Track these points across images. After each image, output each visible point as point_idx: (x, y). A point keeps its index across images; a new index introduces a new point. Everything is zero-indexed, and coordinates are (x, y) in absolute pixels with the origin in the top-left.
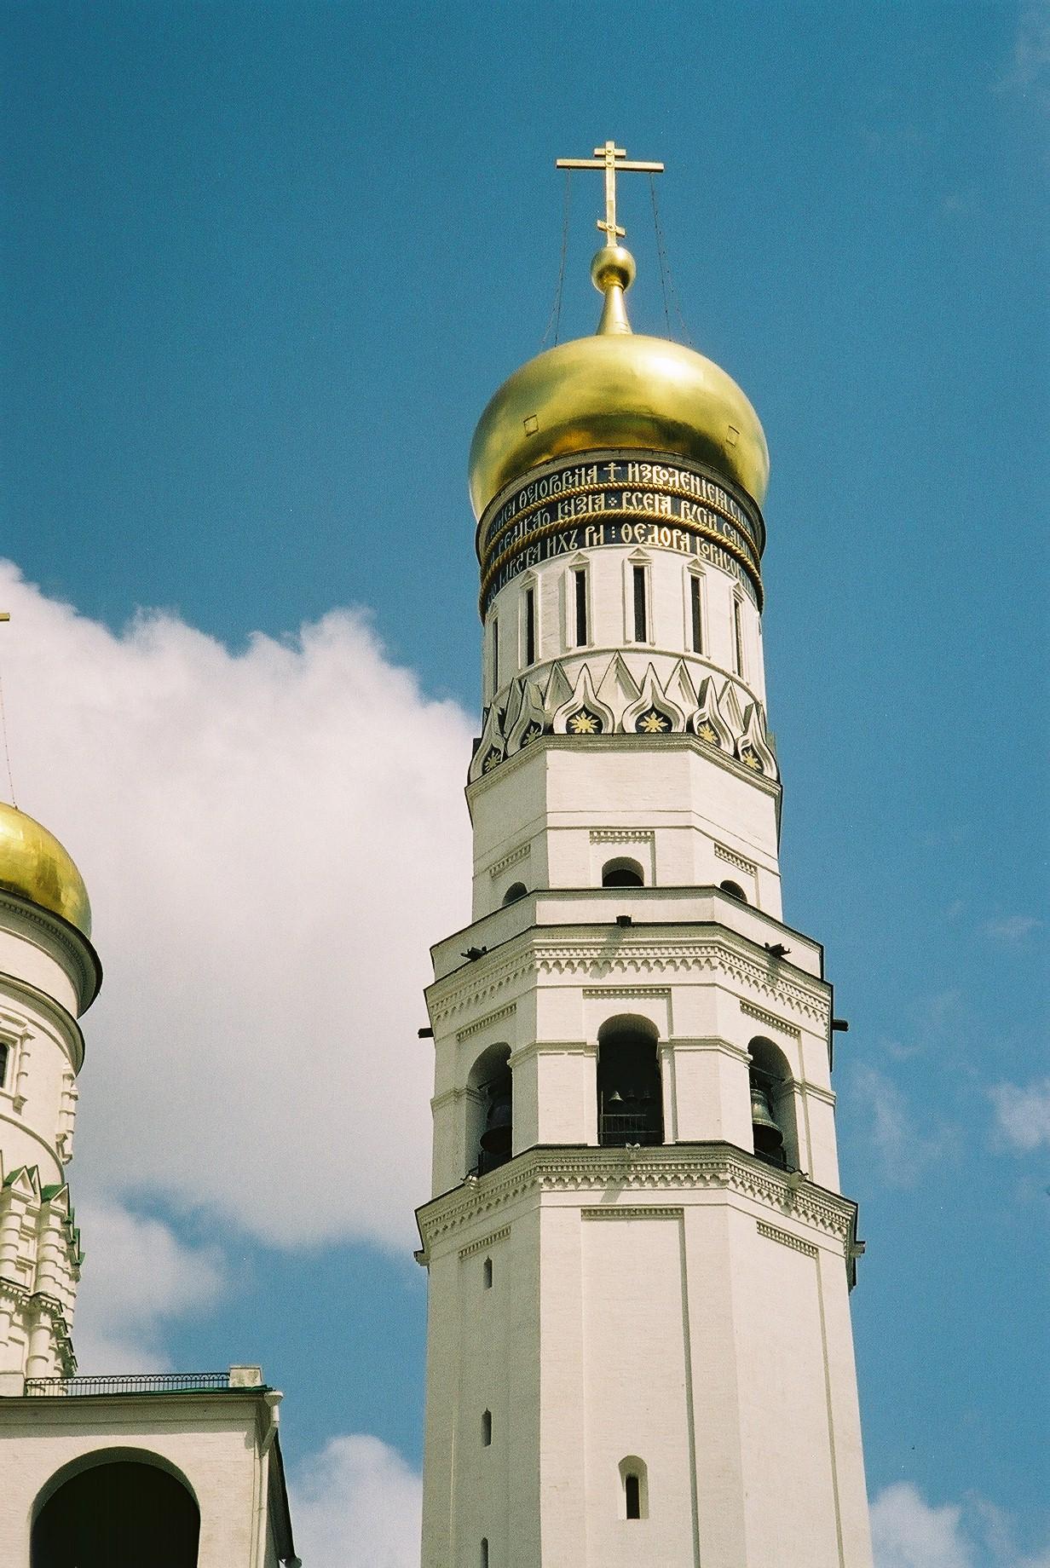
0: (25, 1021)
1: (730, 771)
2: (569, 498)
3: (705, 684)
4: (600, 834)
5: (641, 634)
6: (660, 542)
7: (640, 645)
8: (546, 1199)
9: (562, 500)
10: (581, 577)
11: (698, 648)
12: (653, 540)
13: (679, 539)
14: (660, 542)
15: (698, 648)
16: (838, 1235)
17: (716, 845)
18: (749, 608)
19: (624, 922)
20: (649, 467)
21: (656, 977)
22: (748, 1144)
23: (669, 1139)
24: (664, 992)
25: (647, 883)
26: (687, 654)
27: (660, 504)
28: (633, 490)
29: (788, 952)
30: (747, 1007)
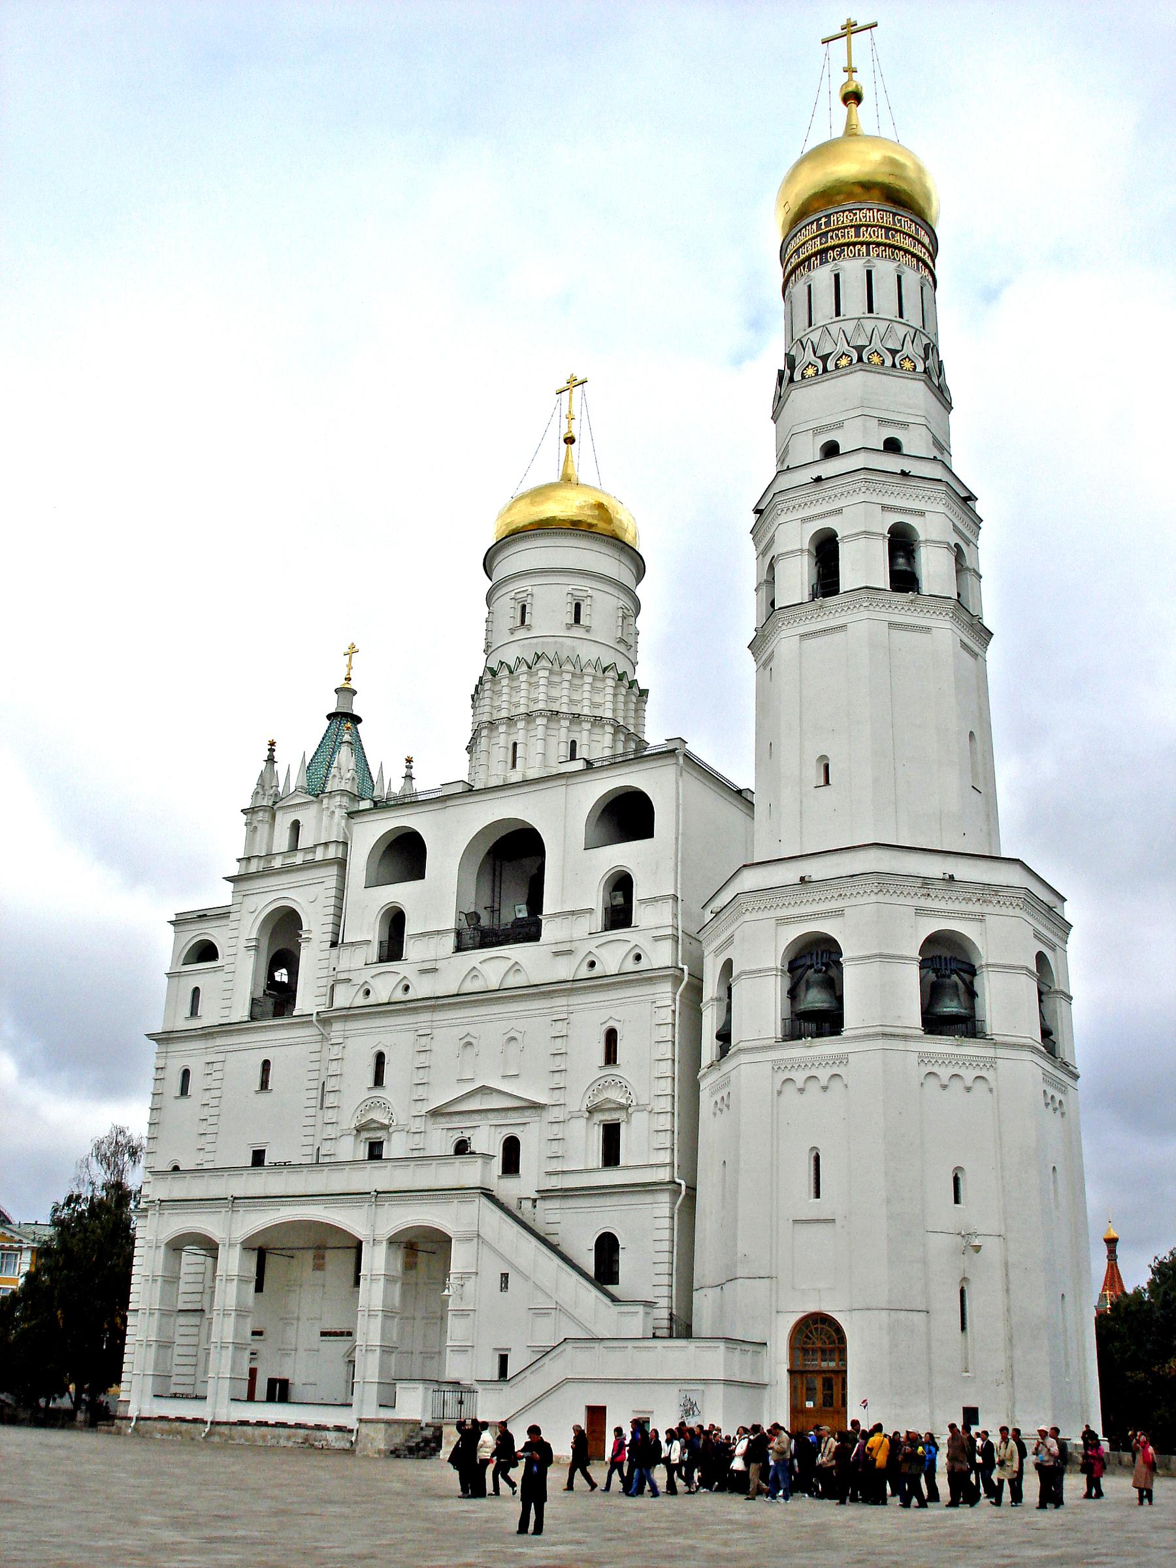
0: (588, 589)
2: (804, 244)
4: (817, 431)
5: (838, 314)
6: (848, 255)
7: (838, 318)
8: (783, 634)
9: (800, 247)
10: (810, 287)
11: (870, 310)
13: (859, 250)
14: (848, 255)
15: (870, 310)
16: (947, 618)
19: (818, 479)
20: (842, 214)
22: (884, 582)
24: (839, 511)
30: (884, 508)
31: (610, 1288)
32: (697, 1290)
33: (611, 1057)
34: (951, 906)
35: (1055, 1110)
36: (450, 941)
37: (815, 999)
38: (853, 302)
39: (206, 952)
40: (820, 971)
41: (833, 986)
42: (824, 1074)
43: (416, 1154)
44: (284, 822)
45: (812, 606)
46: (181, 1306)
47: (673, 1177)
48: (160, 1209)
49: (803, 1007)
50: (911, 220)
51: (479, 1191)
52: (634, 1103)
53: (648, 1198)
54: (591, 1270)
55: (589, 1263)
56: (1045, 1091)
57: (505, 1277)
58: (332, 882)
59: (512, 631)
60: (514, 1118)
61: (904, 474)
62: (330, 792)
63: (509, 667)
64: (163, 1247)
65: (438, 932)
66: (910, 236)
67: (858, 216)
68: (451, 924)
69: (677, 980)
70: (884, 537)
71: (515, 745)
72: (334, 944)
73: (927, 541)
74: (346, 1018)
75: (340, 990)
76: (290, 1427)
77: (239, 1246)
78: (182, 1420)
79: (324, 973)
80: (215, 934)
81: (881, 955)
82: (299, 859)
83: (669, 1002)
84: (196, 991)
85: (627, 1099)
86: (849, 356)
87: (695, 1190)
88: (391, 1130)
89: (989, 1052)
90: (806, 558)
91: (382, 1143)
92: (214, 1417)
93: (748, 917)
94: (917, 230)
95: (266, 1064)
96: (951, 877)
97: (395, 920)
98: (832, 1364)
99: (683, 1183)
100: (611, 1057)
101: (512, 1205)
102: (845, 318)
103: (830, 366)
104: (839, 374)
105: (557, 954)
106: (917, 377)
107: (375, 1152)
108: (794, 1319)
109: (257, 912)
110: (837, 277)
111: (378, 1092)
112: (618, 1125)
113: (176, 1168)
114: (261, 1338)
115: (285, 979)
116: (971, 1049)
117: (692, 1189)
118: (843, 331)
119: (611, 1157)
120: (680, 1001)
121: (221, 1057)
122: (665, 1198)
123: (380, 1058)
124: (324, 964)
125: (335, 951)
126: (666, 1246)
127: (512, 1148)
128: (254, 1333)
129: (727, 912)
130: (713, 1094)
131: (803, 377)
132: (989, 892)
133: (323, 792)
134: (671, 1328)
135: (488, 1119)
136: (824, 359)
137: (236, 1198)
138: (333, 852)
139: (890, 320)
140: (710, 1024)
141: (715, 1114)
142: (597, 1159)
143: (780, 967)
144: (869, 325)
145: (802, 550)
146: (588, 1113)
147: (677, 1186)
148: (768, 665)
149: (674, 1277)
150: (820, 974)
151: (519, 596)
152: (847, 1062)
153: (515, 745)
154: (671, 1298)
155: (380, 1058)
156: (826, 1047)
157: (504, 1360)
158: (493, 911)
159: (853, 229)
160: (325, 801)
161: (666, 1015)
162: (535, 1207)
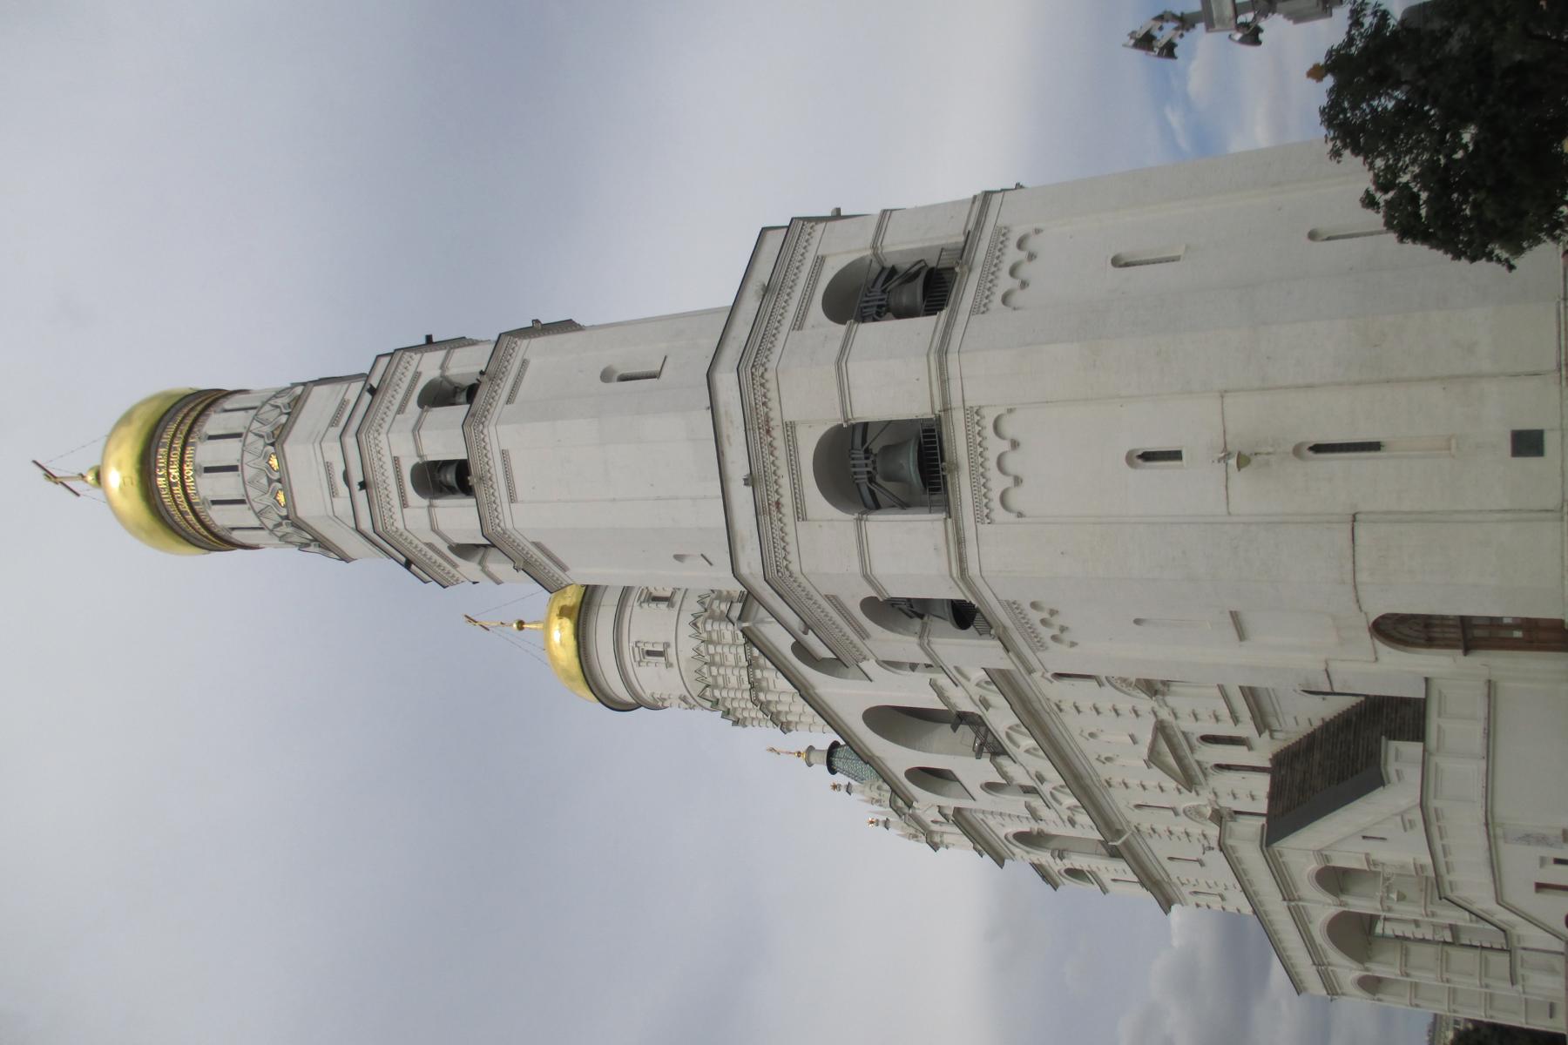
3: (256, 435)
4: (333, 493)
5: (233, 468)
7: (240, 468)
18: (228, 404)
19: (363, 485)
21: (389, 466)
24: (396, 460)
29: (371, 385)
30: (401, 410)
38: (227, 452)
45: (480, 490)
90: (438, 502)
103: (276, 476)
116: (980, 254)
130: (1043, 647)
143: (856, 515)
144: (251, 438)
145: (431, 506)
156: (958, 444)
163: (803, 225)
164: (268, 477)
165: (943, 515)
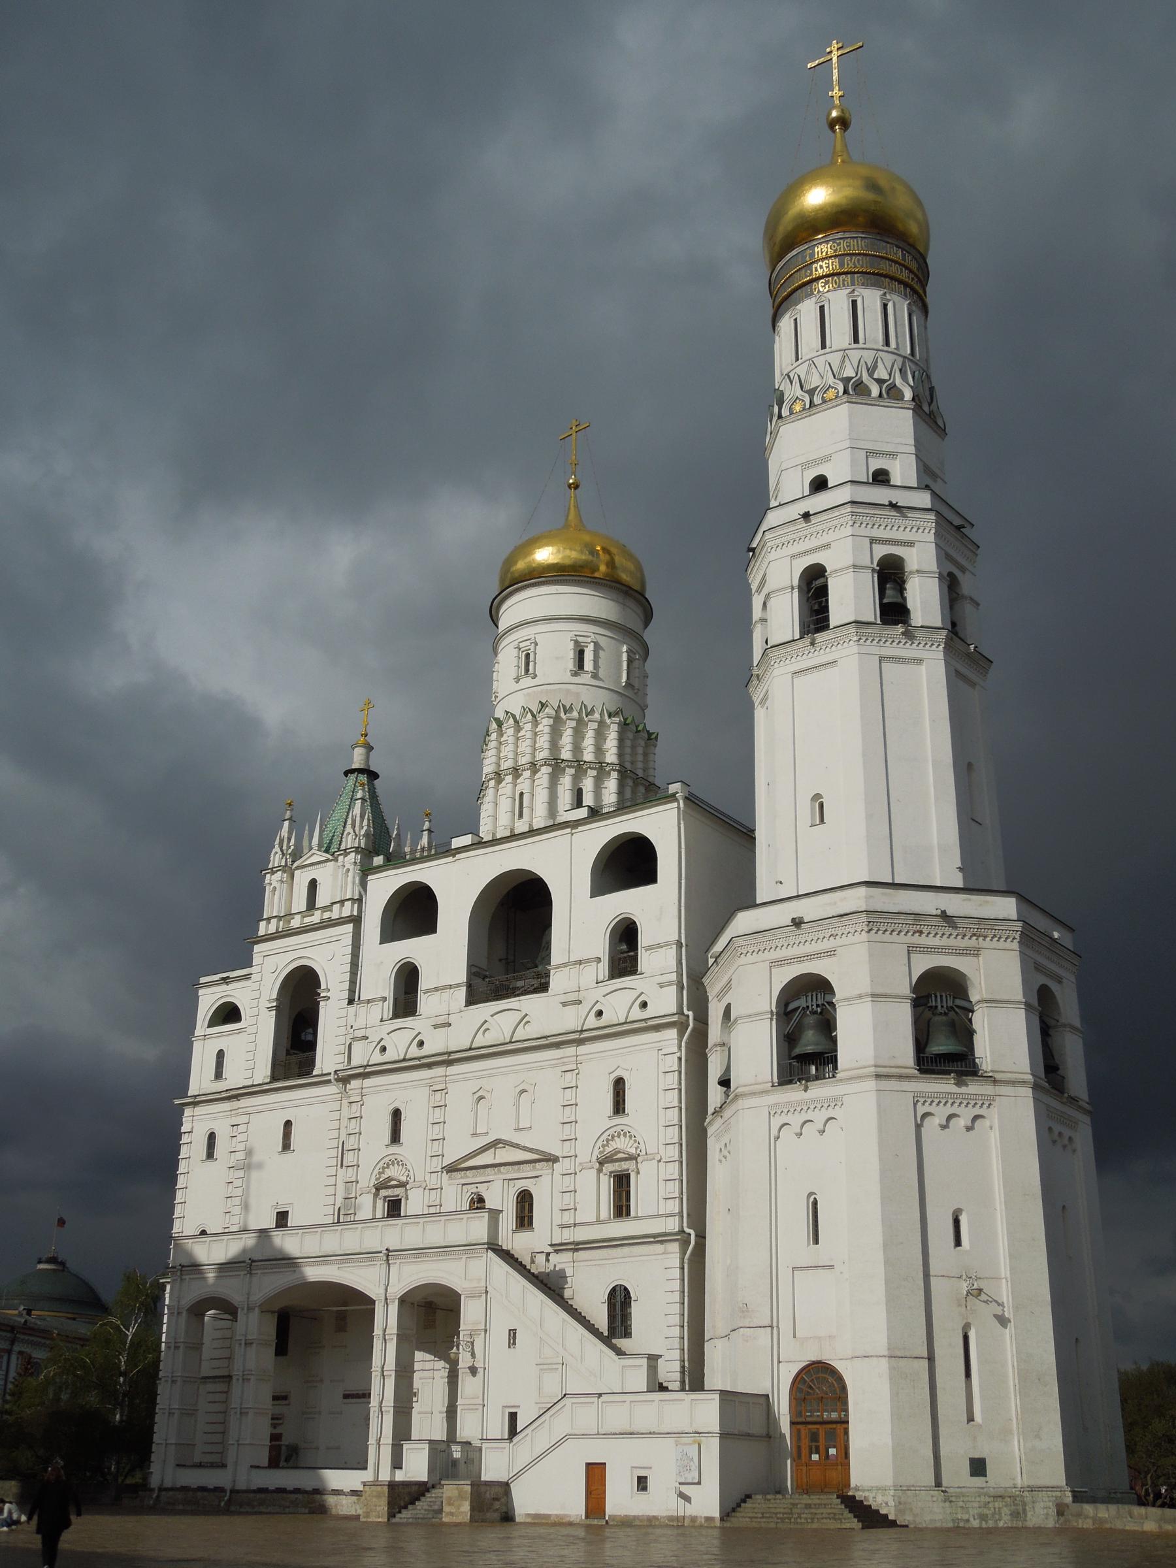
1: (878, 406)
4: (805, 466)
5: (824, 346)
6: (833, 286)
8: (776, 672)
10: (796, 320)
11: (856, 340)
12: (829, 287)
13: (844, 280)
15: (856, 340)
17: (867, 452)
19: (806, 516)
23: (831, 627)
24: (827, 546)
25: (829, 486)
26: (850, 347)
27: (832, 265)
28: (816, 262)
29: (897, 503)
31: (621, 1343)
32: (708, 1341)
33: (619, 1106)
34: (945, 942)
35: (1065, 1147)
36: (462, 993)
37: (810, 1041)
38: (840, 333)
39: (228, 1014)
40: (815, 1013)
41: (827, 1025)
42: (819, 1117)
43: (432, 1210)
44: (302, 879)
46: (204, 1373)
47: (683, 1227)
48: (181, 1274)
49: (798, 1051)
50: (897, 246)
51: (486, 1246)
52: (643, 1152)
53: (659, 1248)
54: (602, 1323)
55: (600, 1318)
56: (1050, 1129)
57: (513, 1334)
58: (348, 940)
59: (517, 680)
60: (527, 1171)
61: (893, 506)
62: (345, 850)
63: (514, 716)
64: (184, 1314)
65: (451, 987)
66: (896, 262)
67: (842, 245)
68: (461, 976)
69: (682, 1027)
70: (873, 570)
71: (522, 794)
72: (351, 1002)
73: (918, 571)
74: (365, 1075)
75: (357, 1047)
76: (306, 1492)
77: (257, 1309)
78: (203, 1489)
79: (343, 1031)
80: (238, 994)
81: (873, 995)
82: (316, 917)
83: (676, 1049)
84: (221, 1055)
85: (636, 1149)
86: (836, 389)
87: (705, 1238)
88: (408, 1187)
89: (988, 1089)
90: (796, 593)
91: (401, 1199)
92: (234, 1486)
93: (743, 960)
94: (904, 255)
95: (288, 1124)
96: (944, 912)
97: (408, 978)
98: (834, 1415)
99: (692, 1232)
100: (619, 1106)
101: (526, 1261)
102: (830, 350)
103: (817, 400)
104: (826, 407)
105: (565, 1004)
106: (906, 406)
107: (394, 1208)
108: (795, 1369)
109: (277, 973)
110: (822, 308)
111: (395, 1149)
112: (628, 1176)
113: (203, 1233)
114: (286, 1402)
115: (309, 1037)
117: (701, 1237)
118: (829, 364)
119: (622, 1209)
120: (686, 1047)
121: (245, 1119)
122: (675, 1247)
123: (396, 1115)
124: (343, 1022)
125: (352, 1008)
126: (676, 1297)
127: (525, 1200)
128: (275, 1398)
129: (725, 956)
131: (791, 413)
132: (983, 926)
133: (339, 850)
134: (683, 1382)
135: (502, 1173)
136: (811, 393)
137: (253, 1261)
138: (348, 910)
139: (877, 350)
140: (714, 1073)
141: (720, 1161)
142: (606, 1208)
144: (855, 355)
146: (598, 1164)
147: (685, 1235)
148: (765, 703)
149: (686, 1328)
150: (815, 1015)
151: (522, 645)
152: (842, 1105)
153: (522, 794)
154: (683, 1350)
155: (396, 1115)
156: (819, 1090)
157: (513, 1417)
158: (507, 963)
159: (837, 259)
160: (341, 858)
161: (672, 1063)
162: (547, 1260)
163: (1017, 931)
164: (819, 386)
165: (775, 1079)
